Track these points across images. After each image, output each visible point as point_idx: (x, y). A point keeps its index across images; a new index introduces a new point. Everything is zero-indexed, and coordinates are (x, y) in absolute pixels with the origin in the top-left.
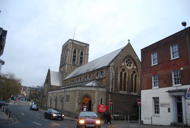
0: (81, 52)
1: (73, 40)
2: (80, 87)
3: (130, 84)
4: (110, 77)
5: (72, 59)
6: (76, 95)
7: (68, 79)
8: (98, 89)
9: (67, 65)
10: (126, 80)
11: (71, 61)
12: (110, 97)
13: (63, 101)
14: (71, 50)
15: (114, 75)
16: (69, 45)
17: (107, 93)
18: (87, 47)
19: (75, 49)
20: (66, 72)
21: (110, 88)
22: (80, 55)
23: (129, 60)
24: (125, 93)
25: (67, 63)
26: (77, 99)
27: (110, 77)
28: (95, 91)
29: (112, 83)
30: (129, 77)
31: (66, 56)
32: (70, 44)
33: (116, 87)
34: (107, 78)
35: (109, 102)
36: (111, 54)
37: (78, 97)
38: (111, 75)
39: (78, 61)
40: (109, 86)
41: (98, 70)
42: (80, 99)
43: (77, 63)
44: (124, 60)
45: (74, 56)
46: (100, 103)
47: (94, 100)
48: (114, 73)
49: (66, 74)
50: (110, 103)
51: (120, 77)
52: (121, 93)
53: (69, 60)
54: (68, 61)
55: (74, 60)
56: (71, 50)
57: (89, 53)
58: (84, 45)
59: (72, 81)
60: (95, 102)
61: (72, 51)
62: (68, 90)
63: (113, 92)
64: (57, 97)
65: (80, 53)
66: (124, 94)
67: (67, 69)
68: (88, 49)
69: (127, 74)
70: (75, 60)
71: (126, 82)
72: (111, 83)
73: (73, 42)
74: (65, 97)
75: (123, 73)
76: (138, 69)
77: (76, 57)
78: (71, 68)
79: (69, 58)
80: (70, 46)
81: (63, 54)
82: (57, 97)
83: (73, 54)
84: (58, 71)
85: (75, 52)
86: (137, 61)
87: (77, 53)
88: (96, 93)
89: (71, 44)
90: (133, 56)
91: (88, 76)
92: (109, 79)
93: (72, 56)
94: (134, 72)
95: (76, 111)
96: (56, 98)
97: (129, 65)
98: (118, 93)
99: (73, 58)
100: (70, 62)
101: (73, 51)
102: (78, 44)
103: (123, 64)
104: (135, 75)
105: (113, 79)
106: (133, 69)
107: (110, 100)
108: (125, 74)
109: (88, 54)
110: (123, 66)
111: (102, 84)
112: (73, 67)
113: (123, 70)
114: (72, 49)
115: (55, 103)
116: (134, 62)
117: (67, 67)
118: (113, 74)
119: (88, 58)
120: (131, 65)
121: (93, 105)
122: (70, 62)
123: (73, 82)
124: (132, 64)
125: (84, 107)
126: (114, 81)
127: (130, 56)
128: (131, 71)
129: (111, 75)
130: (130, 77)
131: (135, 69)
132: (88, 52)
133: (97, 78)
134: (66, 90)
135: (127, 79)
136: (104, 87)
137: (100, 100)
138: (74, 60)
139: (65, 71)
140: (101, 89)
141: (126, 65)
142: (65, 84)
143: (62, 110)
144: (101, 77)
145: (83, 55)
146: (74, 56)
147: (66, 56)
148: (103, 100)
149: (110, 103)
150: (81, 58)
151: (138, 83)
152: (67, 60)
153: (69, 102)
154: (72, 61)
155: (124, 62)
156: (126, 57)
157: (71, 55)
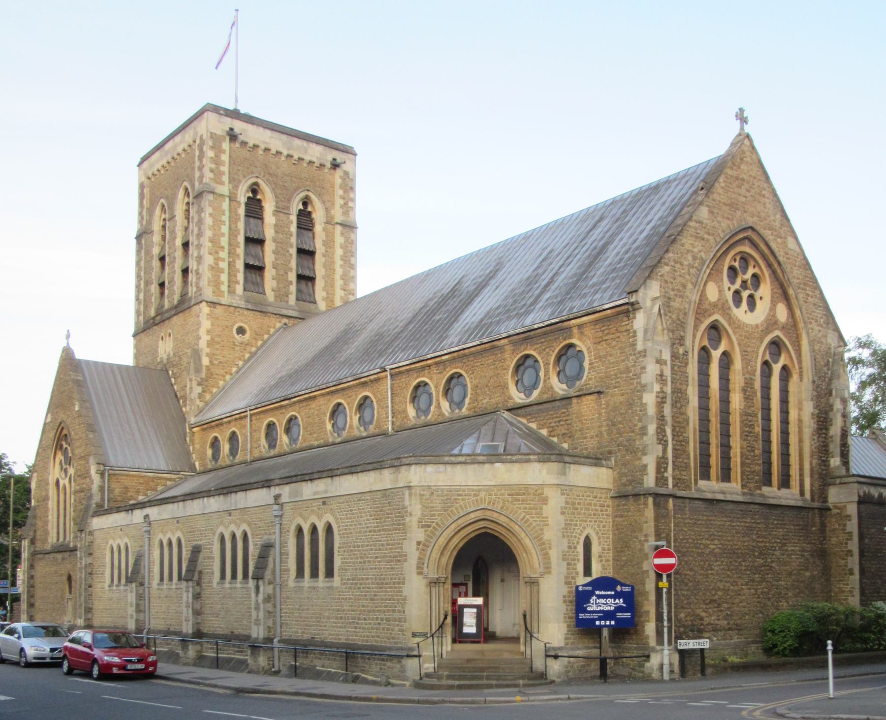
0: (296, 206)
1: (235, 114)
2: (430, 468)
3: (758, 429)
4: (644, 388)
5: (240, 265)
6: (402, 528)
7: (239, 417)
8: (563, 473)
9: (205, 309)
10: (729, 402)
11: (232, 282)
12: (649, 527)
13: (268, 575)
14: (224, 189)
15: (668, 372)
16: (210, 154)
17: (627, 495)
18: (339, 173)
19: (254, 189)
20: (205, 361)
21: (650, 461)
22: (293, 228)
23: (745, 259)
24: (734, 489)
25: (208, 293)
26: (413, 555)
27: (644, 388)
28: (547, 492)
29: (661, 431)
30: (748, 384)
31: (186, 245)
32: (217, 147)
33: (680, 451)
34: (615, 397)
35: (646, 557)
36: (595, 217)
37: (419, 535)
38: (652, 369)
39: (281, 278)
40: (634, 451)
41: (528, 336)
42: (436, 554)
43: (281, 295)
44: (719, 259)
45: (255, 241)
46: (580, 567)
47: (544, 549)
48: (667, 356)
49: (210, 375)
50: (659, 561)
51: (700, 380)
52: (709, 496)
53: (216, 264)
54: (217, 284)
55: (255, 269)
56: (224, 189)
57: (361, 215)
58: (315, 153)
59: (280, 430)
60: (548, 570)
61: (232, 198)
62: (309, 490)
63: (662, 491)
64: (196, 551)
65: (294, 218)
66: (729, 497)
67: (209, 344)
68: (349, 187)
69: (738, 364)
70: (260, 269)
71: (735, 420)
72: (652, 429)
73: (239, 126)
74: (283, 544)
75: (716, 354)
76: (801, 325)
77: (269, 246)
78: (241, 331)
79: (217, 259)
80: (217, 161)
81: (157, 226)
82: (196, 551)
83: (241, 225)
84: (128, 359)
85: (254, 208)
86: (796, 272)
87: (269, 218)
88: (555, 502)
89: (226, 145)
90: (767, 234)
91: (435, 382)
92: (633, 402)
93: (241, 239)
94: (776, 346)
95: (414, 635)
96: (193, 561)
97: (745, 294)
98: (693, 494)
99: (247, 254)
100: (231, 291)
101: (242, 199)
102: (276, 143)
103: (712, 293)
104: (784, 368)
105: (661, 403)
106: (771, 323)
107: (652, 542)
108: (726, 360)
109: (349, 227)
110: (715, 305)
111: (568, 435)
112: (251, 322)
113: (714, 327)
114: (234, 182)
115: (187, 597)
116: (774, 272)
117: (206, 324)
118: (659, 361)
119: (353, 254)
120: (757, 295)
121: (533, 583)
122: (231, 291)
123: (288, 430)
124: (765, 290)
125: (461, 601)
126: (667, 410)
127: (747, 235)
128: (762, 340)
129: (652, 369)
130: (757, 385)
131: (783, 328)
132: (347, 208)
133: (518, 397)
134: (285, 491)
135: (736, 400)
136: (596, 460)
137: (580, 549)
138: (255, 269)
139: (197, 354)
140: (584, 476)
141: (729, 295)
142: (216, 456)
143: (269, 640)
144: (560, 388)
145: (318, 228)
146: (255, 241)
147: (186, 245)
148: (595, 549)
149: (659, 561)
150: (306, 253)
151: (800, 421)
152: (207, 275)
153: (330, 573)
154: (240, 277)
155: (719, 282)
156: (731, 243)
157: (233, 234)
